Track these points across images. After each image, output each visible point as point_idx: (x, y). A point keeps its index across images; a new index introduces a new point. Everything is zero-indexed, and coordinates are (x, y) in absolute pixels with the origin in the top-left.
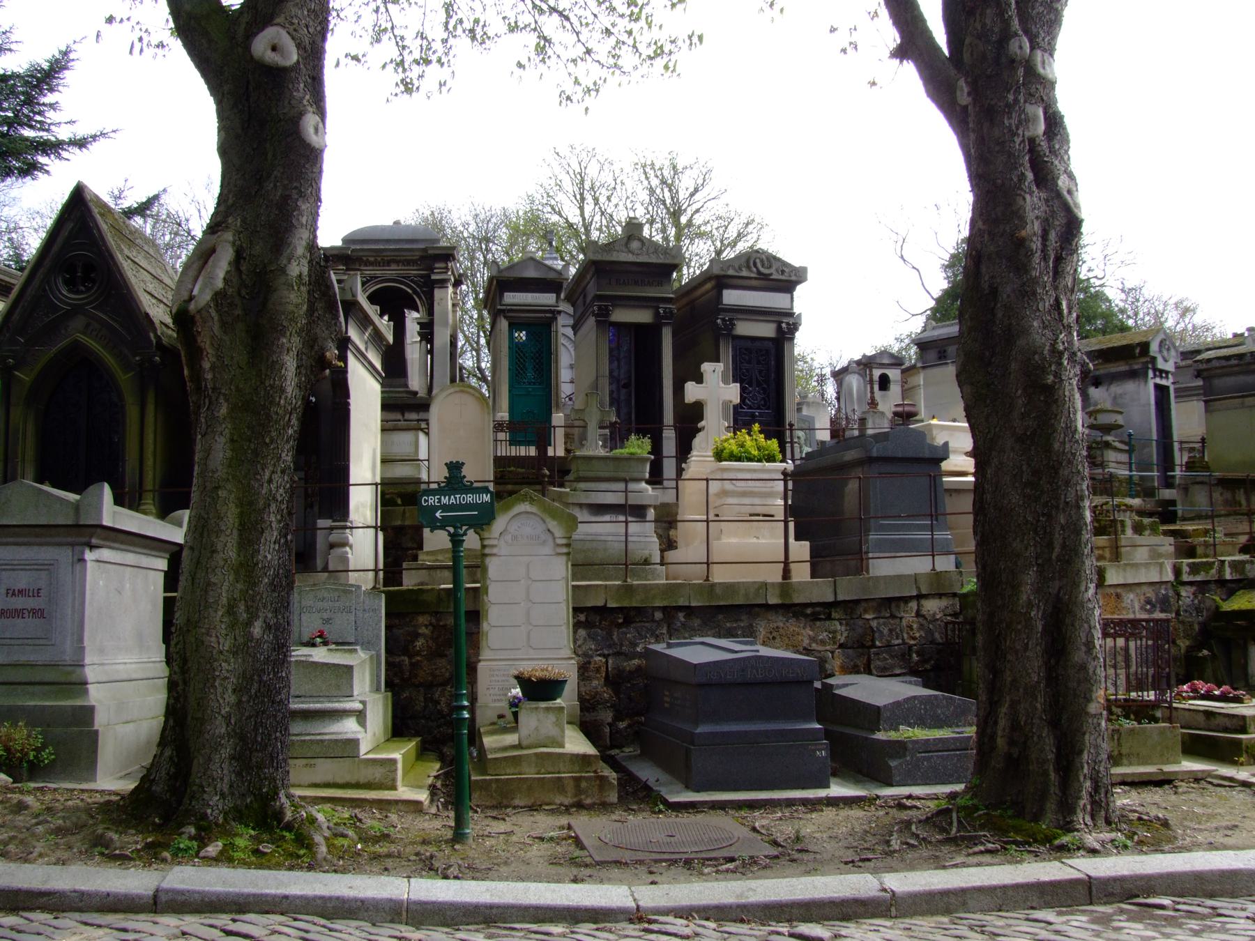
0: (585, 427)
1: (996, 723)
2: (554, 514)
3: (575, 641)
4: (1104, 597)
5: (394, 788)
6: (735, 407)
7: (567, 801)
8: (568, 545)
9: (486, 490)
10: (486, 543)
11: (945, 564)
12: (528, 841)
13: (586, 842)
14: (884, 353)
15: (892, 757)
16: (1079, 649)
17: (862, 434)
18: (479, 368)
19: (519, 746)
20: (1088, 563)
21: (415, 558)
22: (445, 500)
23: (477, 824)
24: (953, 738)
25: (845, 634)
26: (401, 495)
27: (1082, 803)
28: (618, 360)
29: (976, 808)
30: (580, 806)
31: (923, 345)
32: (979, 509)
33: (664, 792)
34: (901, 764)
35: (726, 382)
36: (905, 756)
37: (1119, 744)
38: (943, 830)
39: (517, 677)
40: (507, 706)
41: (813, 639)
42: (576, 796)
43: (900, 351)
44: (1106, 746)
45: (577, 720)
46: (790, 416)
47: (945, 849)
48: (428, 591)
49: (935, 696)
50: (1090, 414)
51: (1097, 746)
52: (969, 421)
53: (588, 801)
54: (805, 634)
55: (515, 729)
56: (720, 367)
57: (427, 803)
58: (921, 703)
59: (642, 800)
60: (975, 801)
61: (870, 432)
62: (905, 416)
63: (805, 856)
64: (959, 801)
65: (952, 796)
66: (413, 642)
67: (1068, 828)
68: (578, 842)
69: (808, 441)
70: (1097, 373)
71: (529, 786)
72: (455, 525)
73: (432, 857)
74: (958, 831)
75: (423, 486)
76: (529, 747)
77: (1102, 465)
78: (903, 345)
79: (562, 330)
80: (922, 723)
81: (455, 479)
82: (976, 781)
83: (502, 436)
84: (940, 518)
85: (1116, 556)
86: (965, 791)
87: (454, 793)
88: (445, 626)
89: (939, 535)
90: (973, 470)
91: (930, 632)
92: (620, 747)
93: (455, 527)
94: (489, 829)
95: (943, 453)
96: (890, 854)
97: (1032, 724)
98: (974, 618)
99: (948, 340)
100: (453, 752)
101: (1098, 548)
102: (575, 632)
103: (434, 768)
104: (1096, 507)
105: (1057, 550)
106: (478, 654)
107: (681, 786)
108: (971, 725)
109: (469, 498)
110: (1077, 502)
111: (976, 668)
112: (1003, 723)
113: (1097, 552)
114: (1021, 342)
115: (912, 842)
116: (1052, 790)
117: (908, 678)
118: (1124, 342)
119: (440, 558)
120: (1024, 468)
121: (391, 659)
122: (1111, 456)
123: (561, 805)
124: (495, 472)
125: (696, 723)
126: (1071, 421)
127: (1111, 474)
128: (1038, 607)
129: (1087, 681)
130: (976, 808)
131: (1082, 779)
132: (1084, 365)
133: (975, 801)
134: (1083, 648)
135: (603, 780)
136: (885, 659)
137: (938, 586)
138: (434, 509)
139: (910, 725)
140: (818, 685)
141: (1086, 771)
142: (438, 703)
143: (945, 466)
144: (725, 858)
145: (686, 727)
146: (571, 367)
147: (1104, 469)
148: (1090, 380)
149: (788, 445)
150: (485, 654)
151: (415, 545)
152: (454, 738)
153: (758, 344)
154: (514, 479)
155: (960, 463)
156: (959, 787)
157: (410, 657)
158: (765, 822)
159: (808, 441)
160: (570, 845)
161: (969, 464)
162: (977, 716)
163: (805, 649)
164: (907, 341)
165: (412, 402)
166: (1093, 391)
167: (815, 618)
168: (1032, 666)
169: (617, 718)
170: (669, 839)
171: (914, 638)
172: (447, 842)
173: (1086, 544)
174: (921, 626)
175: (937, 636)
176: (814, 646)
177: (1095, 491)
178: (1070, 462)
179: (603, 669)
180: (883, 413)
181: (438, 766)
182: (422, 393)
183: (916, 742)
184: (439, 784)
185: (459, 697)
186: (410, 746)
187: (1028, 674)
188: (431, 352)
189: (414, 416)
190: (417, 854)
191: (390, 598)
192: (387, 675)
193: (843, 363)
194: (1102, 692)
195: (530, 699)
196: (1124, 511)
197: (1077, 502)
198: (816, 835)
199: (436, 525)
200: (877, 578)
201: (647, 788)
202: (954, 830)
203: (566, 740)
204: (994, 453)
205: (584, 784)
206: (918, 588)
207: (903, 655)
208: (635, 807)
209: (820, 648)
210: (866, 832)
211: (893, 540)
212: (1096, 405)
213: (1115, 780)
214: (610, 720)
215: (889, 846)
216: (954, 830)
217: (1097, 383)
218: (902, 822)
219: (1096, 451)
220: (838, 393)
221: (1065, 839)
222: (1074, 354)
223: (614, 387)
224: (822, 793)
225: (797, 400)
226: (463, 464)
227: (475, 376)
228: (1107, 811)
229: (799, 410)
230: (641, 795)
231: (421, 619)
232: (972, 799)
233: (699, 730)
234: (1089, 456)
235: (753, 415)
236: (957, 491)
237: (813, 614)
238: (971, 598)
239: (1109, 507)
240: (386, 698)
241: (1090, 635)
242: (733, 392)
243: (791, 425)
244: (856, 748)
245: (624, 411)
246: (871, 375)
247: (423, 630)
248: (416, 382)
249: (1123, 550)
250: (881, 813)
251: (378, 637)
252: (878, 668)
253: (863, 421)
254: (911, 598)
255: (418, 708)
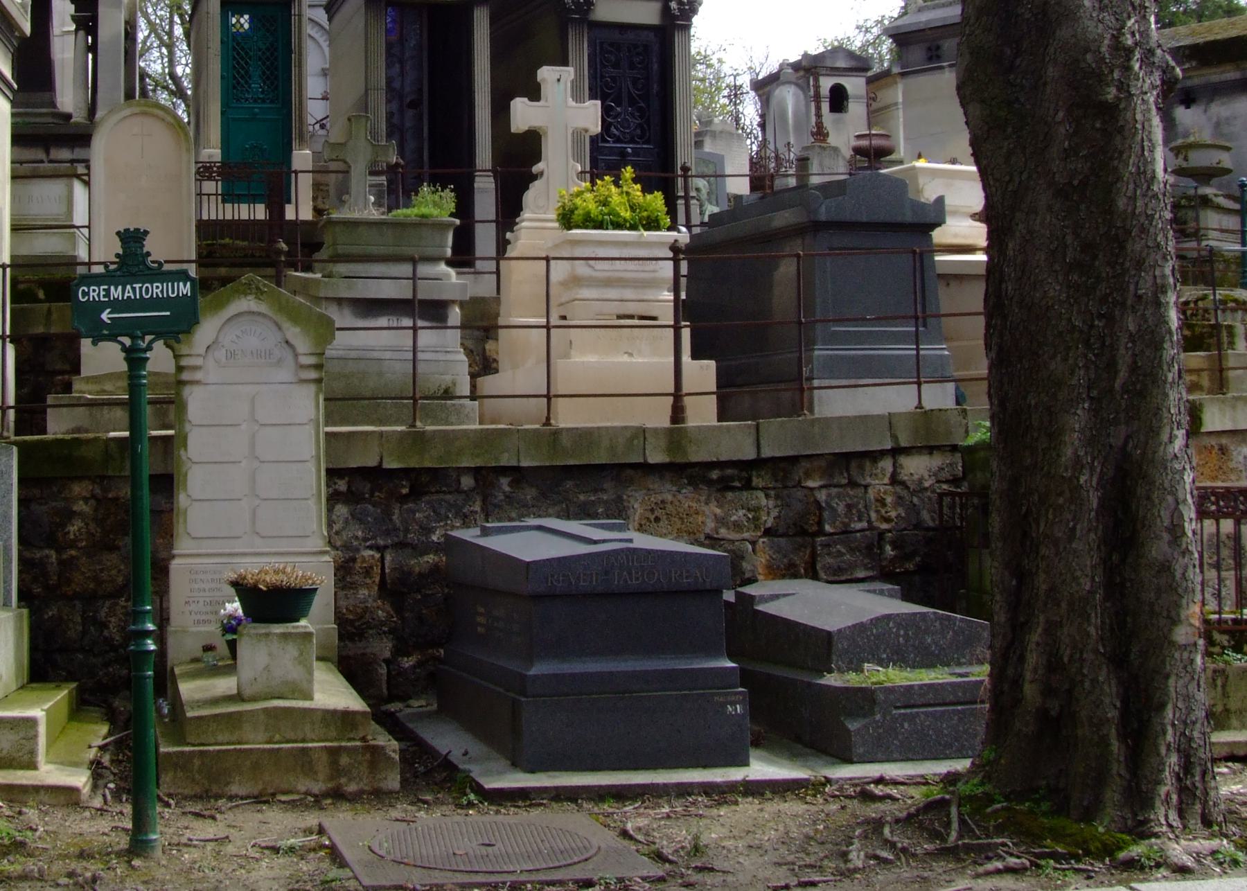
0: (347, 172)
1: (1022, 659)
2: (295, 315)
3: (330, 524)
4: (1200, 453)
5: (32, 765)
6: (594, 140)
7: (317, 788)
8: (318, 367)
9: (183, 276)
10: (184, 362)
11: (939, 397)
12: (253, 853)
13: (348, 854)
14: (838, 50)
15: (852, 715)
16: (1158, 538)
17: (803, 185)
18: (173, 76)
19: (238, 697)
20: (1173, 395)
21: (68, 388)
22: (116, 293)
23: (169, 824)
24: (951, 684)
25: (775, 513)
26: (42, 284)
27: (1163, 790)
28: (401, 62)
29: (989, 799)
30: (338, 795)
31: (902, 37)
32: (995, 307)
33: (476, 772)
34: (866, 727)
35: (578, 98)
36: (873, 714)
37: (1225, 695)
38: (935, 835)
39: (235, 584)
40: (219, 631)
41: (721, 521)
42: (331, 778)
43: (864, 47)
44: (1202, 697)
45: (334, 654)
46: (684, 154)
47: (939, 866)
48: (88, 441)
49: (923, 615)
50: (1177, 151)
51: (1188, 698)
52: (977, 163)
53: (352, 788)
54: (709, 512)
55: (231, 669)
56: (568, 73)
57: (86, 790)
58: (899, 626)
59: (440, 786)
60: (988, 788)
61: (815, 180)
62: (873, 154)
63: (708, 879)
64: (963, 788)
65: (951, 779)
66: (64, 525)
67: (1141, 831)
68: (335, 855)
69: (713, 196)
70: (1189, 83)
71: (256, 762)
72: (134, 333)
73: (95, 879)
74: (960, 837)
75: (81, 270)
76: (254, 699)
77: (1197, 235)
78: (870, 37)
79: (308, 13)
80: (900, 658)
81: (133, 256)
82: (989, 754)
83: (209, 187)
84: (930, 320)
85: (1220, 384)
86: (971, 772)
87: (132, 773)
88: (117, 499)
89: (928, 350)
90: (983, 243)
91: (913, 509)
92: (404, 698)
93: (133, 338)
94: (188, 834)
95: (936, 214)
96: (849, 874)
97: (1082, 660)
98: (986, 487)
99: (945, 29)
100: (130, 707)
101: (1190, 371)
102: (330, 510)
103: (99, 733)
104: (1186, 303)
105: (1123, 374)
106: (170, 546)
107: (504, 763)
108: (980, 662)
109: (157, 289)
110: (1155, 294)
111: (990, 568)
112: (1032, 659)
113: (1188, 378)
114: (1064, 33)
115: (884, 854)
116: (1115, 768)
117: (878, 585)
118: (1233, 33)
119: (108, 387)
120: (1069, 239)
121: (27, 554)
122: (1211, 219)
123: (307, 793)
124: (199, 247)
125: (530, 660)
126: (1146, 163)
127: (1211, 250)
128: (1092, 469)
129: (1172, 592)
130: (989, 799)
131: (1163, 751)
132: (1166, 70)
133: (988, 788)
134: (1166, 537)
135: (376, 752)
136: (840, 554)
137: (927, 433)
138: (99, 306)
139: (881, 663)
140: (729, 596)
141: (1169, 737)
142: (104, 625)
143: (938, 236)
144: (576, 882)
145: (514, 666)
146: (324, 73)
147: (1199, 241)
148: (1177, 95)
149: (681, 202)
150: (183, 546)
151: (67, 367)
152: (131, 685)
153: (631, 36)
154: (227, 259)
155: (963, 232)
156: (962, 765)
157: (59, 551)
158: (642, 822)
159: (713, 196)
160: (321, 860)
161: (978, 233)
162: (991, 647)
163: (708, 537)
164: (876, 31)
165: (63, 131)
166: (1182, 114)
167: (724, 486)
168: (1082, 566)
169: (399, 651)
170: (484, 850)
171: (887, 520)
172: (119, 854)
173: (1170, 365)
174: (899, 500)
175: (925, 515)
176: (723, 532)
177: (1185, 278)
178: (1143, 230)
179: (377, 570)
180: (836, 150)
181: (104, 729)
182: (79, 117)
183: (891, 690)
184: (106, 759)
185: (138, 616)
186: (59, 696)
187: (1075, 579)
188: (93, 49)
189: (65, 154)
190: (71, 875)
191: (27, 454)
192: (21, 581)
193: (771, 67)
194: (1196, 609)
195: (254, 621)
196: (1234, 310)
197: (1155, 294)
198: (726, 843)
199: (101, 334)
200: (827, 422)
201: (448, 765)
202: (954, 835)
203: (316, 686)
204: (1018, 214)
205: (344, 760)
206: (894, 437)
207: (869, 548)
208: (428, 798)
209: (733, 536)
210: (808, 838)
211: (852, 358)
212: (1186, 135)
213: (1218, 752)
214: (387, 654)
215: (847, 861)
216: (954, 835)
217: (1188, 99)
218: (867, 822)
219: (1186, 213)
220: (762, 116)
221: (1136, 850)
222: (1151, 52)
223: (395, 106)
224: (736, 774)
225: (696, 127)
226: (146, 233)
227: (166, 88)
228: (1205, 804)
229: (699, 144)
230: (439, 777)
231: (77, 489)
232: (982, 784)
233: (532, 672)
234: (1175, 220)
235: (622, 153)
236: (958, 277)
237: (721, 479)
238: (982, 454)
239: (1208, 304)
240: (19, 618)
241: (1177, 515)
242: (590, 116)
243: (685, 169)
244: (792, 699)
245: (411, 145)
246: (817, 87)
247: (80, 506)
248: (68, 98)
249: (1231, 374)
250: (834, 807)
251: (7, 517)
252: (827, 569)
253: (803, 162)
254: (882, 453)
255: (72, 634)
